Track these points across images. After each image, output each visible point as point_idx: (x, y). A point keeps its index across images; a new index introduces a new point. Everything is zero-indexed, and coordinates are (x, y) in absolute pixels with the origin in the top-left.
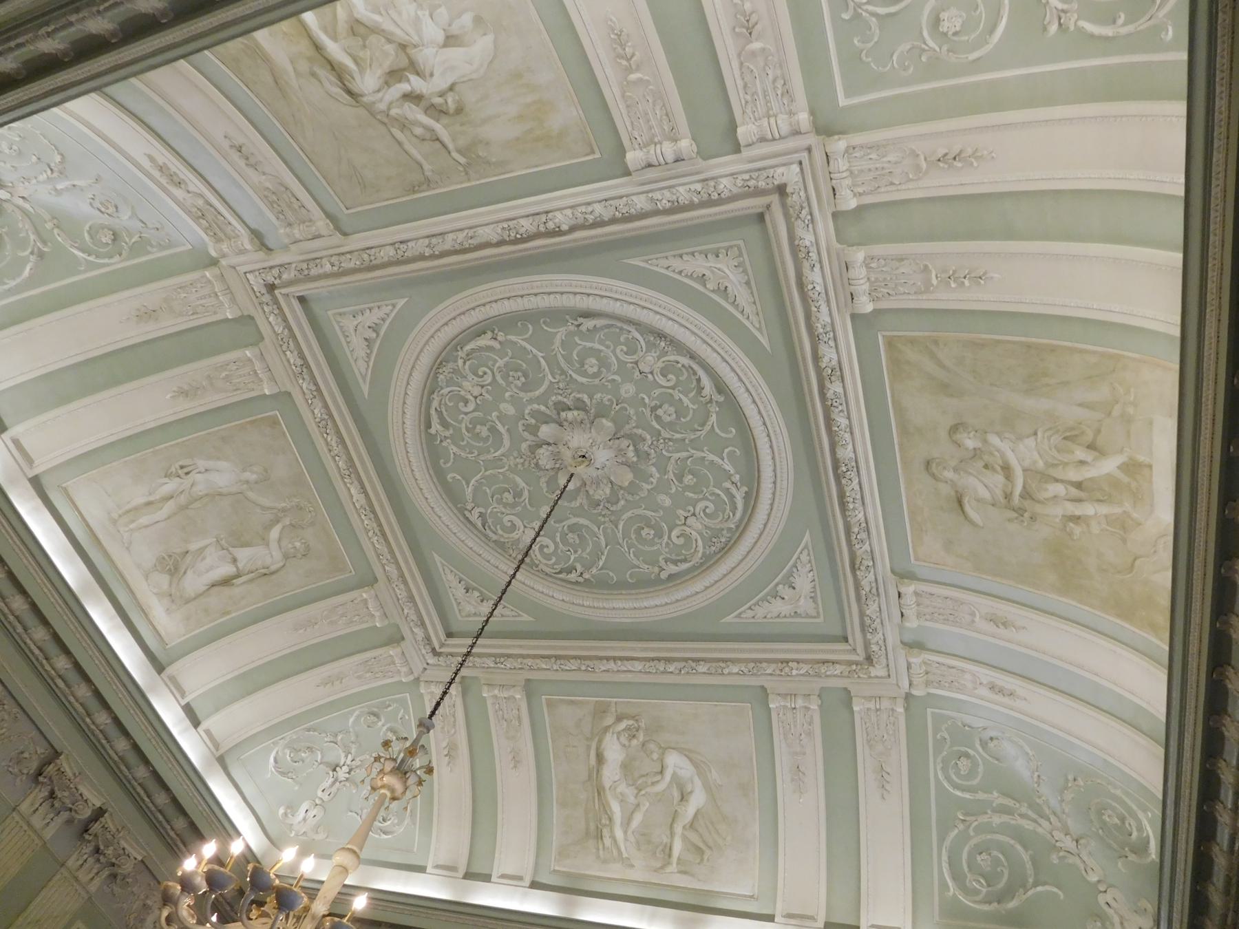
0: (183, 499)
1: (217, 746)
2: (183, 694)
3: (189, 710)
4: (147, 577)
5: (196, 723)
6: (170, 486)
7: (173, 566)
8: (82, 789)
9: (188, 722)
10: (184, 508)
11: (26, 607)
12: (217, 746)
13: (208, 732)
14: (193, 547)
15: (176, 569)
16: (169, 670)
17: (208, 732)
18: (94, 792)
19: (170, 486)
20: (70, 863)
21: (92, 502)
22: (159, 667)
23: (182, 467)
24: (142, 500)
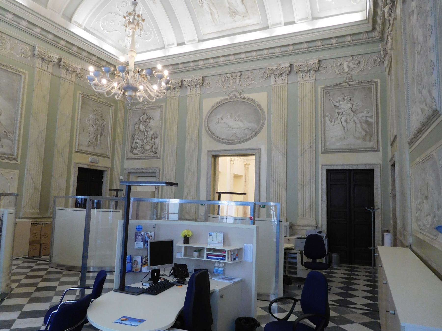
0: (211, 4)
1: (307, 18)
2: (280, 24)
3: (287, 24)
4: (236, 22)
5: (294, 23)
6: (206, 7)
7: (234, 13)
8: (282, 67)
9: (291, 26)
10: (213, 4)
11: (223, 58)
12: (307, 18)
13: (300, 20)
14: (227, 5)
15: (234, 12)
16: (269, 25)
17: (300, 20)
18: (313, 60)
19: (206, 7)
20: (299, 80)
21: (208, 29)
22: (267, 28)
23: (200, 2)
24: (210, 16)
